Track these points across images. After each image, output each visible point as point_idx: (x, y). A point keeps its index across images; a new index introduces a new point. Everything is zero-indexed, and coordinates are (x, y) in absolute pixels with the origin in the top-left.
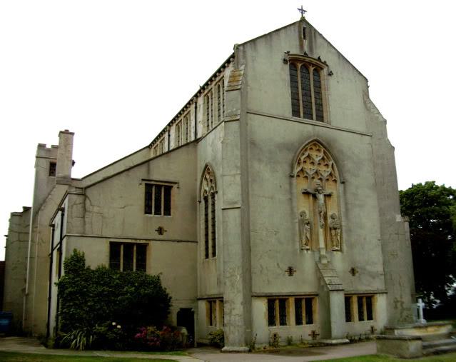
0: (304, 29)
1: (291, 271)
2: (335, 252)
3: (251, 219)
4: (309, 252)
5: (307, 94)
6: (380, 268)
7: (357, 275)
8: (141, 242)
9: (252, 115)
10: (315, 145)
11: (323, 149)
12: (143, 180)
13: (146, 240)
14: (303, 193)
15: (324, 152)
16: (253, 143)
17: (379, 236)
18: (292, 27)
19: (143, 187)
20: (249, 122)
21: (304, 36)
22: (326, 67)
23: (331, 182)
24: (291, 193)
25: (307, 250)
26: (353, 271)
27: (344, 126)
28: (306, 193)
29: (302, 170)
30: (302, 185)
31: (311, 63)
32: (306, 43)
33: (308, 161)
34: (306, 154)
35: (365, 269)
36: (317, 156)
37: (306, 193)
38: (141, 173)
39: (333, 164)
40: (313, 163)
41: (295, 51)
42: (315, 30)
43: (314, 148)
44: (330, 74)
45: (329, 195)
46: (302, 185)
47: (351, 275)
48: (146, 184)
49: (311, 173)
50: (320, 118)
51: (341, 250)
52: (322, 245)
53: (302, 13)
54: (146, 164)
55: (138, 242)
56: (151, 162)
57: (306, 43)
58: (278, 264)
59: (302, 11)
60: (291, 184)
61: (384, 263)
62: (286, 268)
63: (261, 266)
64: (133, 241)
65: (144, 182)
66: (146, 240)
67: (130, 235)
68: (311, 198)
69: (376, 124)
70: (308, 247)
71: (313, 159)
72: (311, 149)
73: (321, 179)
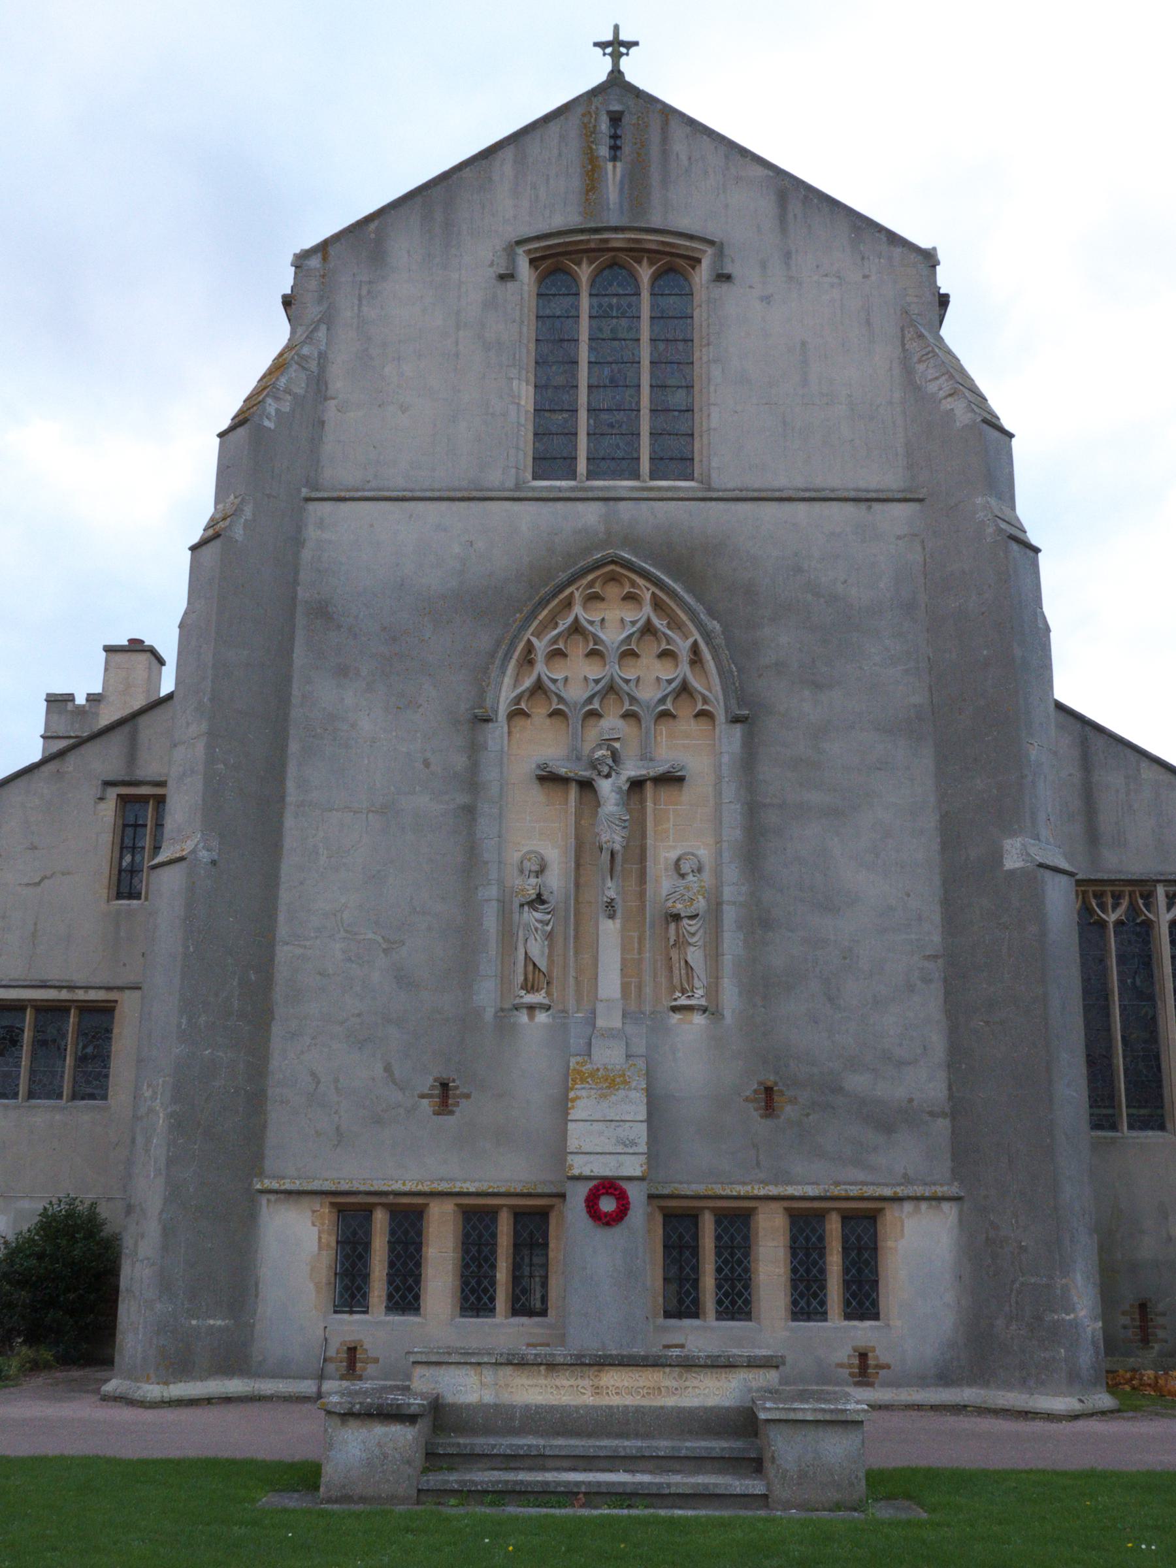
0: (618, 122)
1: (445, 1095)
2: (677, 1017)
3: (285, 896)
4: (542, 1017)
5: (615, 378)
6: (927, 1083)
7: (789, 1111)
8: (93, 995)
9: (328, 506)
10: (613, 578)
11: (647, 593)
12: (108, 784)
13: (109, 989)
14: (542, 779)
15: (657, 605)
16: (323, 612)
17: (937, 939)
18: (554, 127)
19: (108, 810)
20: (312, 533)
21: (615, 148)
22: (710, 251)
23: (687, 725)
24: (471, 781)
25: (531, 1008)
26: (768, 1099)
27: (781, 479)
28: (549, 779)
29: (539, 688)
30: (542, 744)
31: (638, 252)
32: (613, 174)
33: (577, 650)
34: (564, 624)
35: (839, 1090)
36: (613, 622)
37: (549, 779)
38: (104, 760)
39: (695, 644)
40: (593, 654)
41: (560, 214)
42: (668, 113)
43: (613, 592)
44: (724, 278)
45: (672, 779)
46: (542, 744)
47: (755, 1115)
48: (123, 799)
49: (576, 693)
50: (676, 459)
51: (710, 1010)
52: (610, 983)
53: (616, 57)
54: (126, 729)
55: (80, 995)
56: (143, 721)
57: (613, 174)
58: (388, 1069)
59: (617, 47)
60: (474, 749)
61: (958, 1058)
62: (426, 1083)
63: (313, 1074)
64: (64, 995)
65: (112, 793)
66: (109, 989)
67: (53, 974)
68: (573, 792)
69: (959, 452)
70: (530, 998)
71: (597, 640)
72: (596, 598)
73: (628, 715)
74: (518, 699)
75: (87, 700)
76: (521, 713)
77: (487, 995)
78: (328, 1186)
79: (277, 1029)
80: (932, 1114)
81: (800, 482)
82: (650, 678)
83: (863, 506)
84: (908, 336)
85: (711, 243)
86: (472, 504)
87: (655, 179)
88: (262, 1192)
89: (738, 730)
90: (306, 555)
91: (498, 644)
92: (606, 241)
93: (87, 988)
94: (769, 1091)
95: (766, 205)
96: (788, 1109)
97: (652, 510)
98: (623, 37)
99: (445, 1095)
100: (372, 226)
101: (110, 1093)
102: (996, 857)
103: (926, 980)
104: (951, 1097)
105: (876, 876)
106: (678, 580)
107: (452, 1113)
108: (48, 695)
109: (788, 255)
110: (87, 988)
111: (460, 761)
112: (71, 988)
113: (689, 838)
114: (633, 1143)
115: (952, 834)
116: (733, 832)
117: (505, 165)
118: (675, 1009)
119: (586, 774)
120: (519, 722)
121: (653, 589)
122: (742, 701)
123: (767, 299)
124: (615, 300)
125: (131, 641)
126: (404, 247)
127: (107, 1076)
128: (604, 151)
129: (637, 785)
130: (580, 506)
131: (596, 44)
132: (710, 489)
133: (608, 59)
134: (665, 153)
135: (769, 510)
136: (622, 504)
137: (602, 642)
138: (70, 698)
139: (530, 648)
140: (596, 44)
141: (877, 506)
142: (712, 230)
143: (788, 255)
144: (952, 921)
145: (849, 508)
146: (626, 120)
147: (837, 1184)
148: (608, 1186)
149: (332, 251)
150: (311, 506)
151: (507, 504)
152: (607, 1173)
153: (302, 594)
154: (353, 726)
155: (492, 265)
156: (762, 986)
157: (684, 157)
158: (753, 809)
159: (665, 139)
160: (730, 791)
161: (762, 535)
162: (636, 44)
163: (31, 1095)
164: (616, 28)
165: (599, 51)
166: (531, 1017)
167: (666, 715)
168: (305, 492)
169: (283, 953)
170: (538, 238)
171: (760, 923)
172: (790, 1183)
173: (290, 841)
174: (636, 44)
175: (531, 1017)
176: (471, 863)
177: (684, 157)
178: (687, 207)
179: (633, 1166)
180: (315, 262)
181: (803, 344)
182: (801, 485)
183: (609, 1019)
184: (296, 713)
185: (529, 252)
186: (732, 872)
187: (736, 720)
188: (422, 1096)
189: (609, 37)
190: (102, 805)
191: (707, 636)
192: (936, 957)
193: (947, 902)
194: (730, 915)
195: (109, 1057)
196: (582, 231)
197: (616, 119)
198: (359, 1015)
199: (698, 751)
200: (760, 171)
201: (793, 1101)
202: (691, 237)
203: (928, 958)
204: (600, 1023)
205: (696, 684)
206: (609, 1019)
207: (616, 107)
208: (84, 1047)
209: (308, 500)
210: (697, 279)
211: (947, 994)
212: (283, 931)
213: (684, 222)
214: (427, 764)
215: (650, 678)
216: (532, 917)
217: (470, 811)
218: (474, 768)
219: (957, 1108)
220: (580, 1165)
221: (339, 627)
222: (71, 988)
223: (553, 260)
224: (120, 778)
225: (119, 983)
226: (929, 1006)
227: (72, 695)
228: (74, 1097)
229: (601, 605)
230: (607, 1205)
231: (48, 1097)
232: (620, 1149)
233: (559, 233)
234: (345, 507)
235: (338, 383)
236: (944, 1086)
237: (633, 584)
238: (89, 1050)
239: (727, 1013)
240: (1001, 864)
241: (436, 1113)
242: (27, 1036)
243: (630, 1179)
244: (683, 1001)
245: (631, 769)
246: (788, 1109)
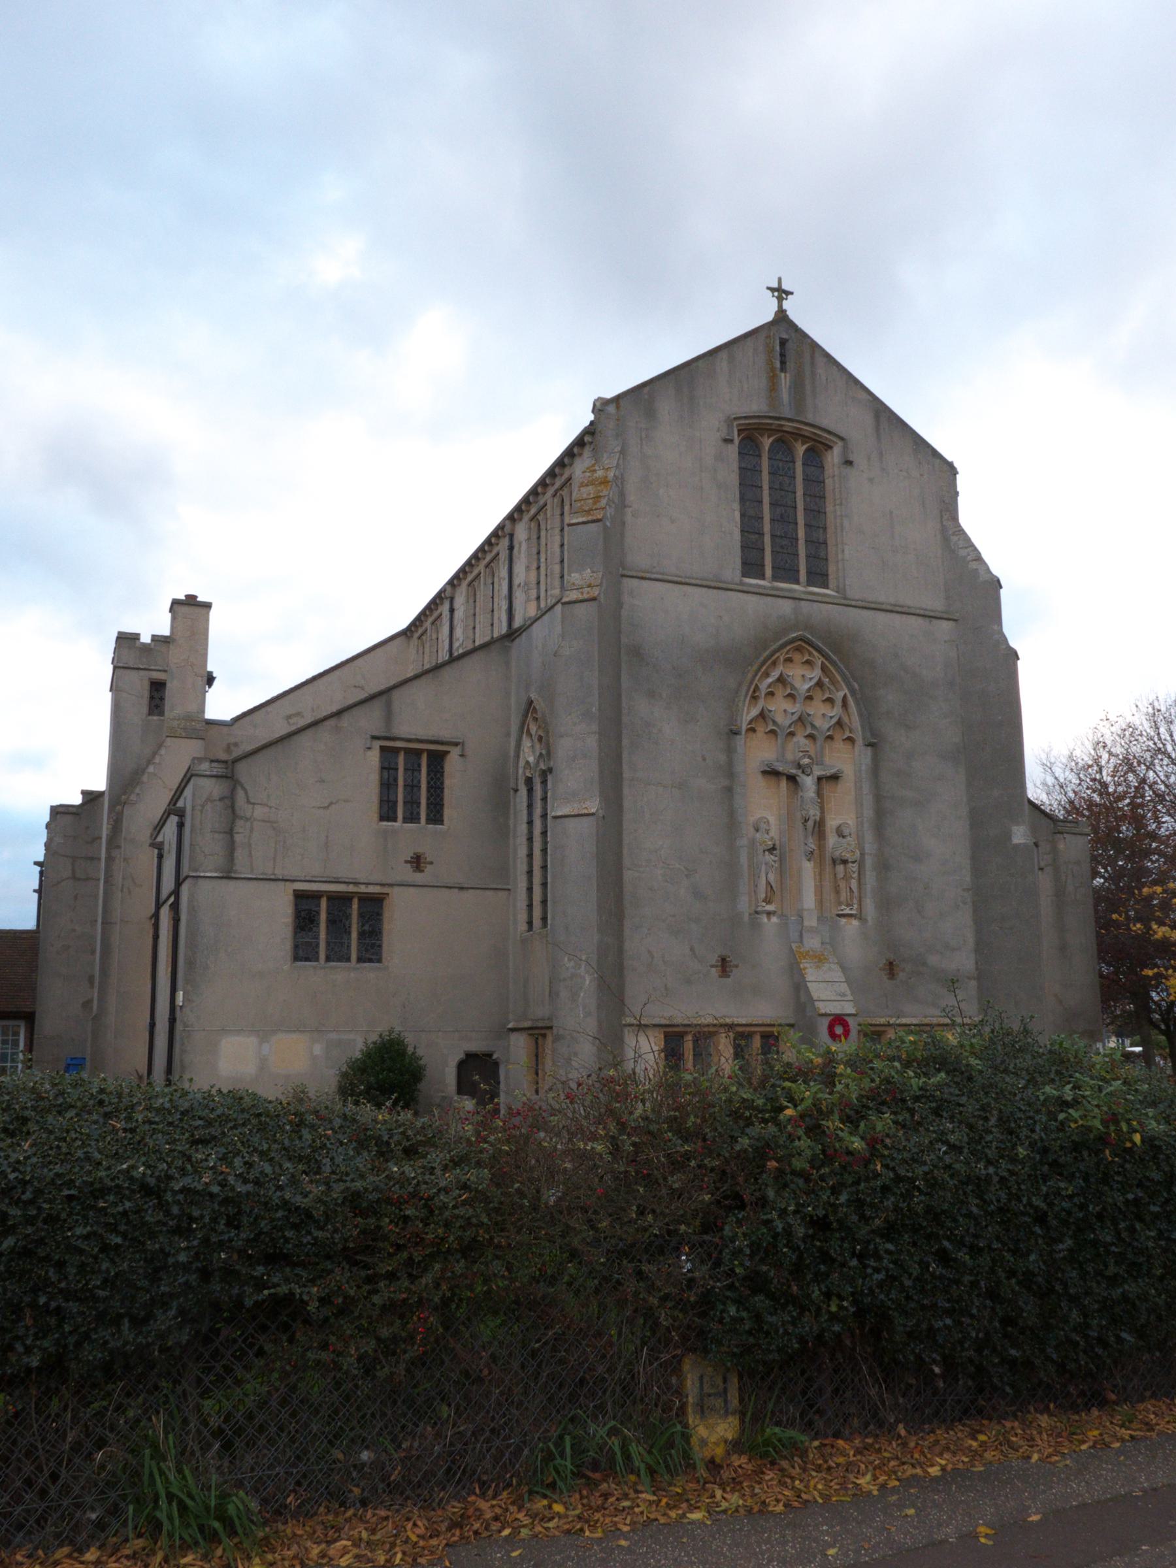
0: (782, 346)
1: (724, 966)
2: (844, 920)
3: (626, 839)
4: (774, 919)
5: (784, 518)
6: (964, 961)
7: (902, 976)
8: (372, 889)
9: (635, 582)
10: (798, 649)
11: (819, 661)
12: (374, 738)
13: (382, 885)
14: (764, 773)
15: (824, 669)
16: (637, 652)
17: (968, 879)
18: (749, 342)
19: (374, 757)
20: (626, 598)
21: (783, 363)
22: (840, 443)
23: (838, 744)
24: (729, 771)
25: (769, 914)
26: (891, 969)
27: (883, 596)
28: (771, 773)
29: (762, 715)
30: (759, 752)
31: (798, 435)
32: (785, 380)
33: (780, 692)
34: (775, 675)
35: (924, 964)
36: (802, 677)
37: (771, 773)
38: (370, 720)
39: (845, 696)
40: (791, 696)
41: (756, 406)
42: (815, 346)
43: (797, 657)
44: (849, 463)
45: (835, 778)
46: (759, 752)
47: (885, 978)
48: (383, 749)
49: (783, 721)
50: (819, 576)
51: (860, 916)
52: (809, 900)
53: (780, 300)
54: (384, 698)
55: (363, 889)
56: (395, 694)
57: (785, 380)
58: (692, 949)
59: (781, 293)
60: (730, 751)
61: (981, 947)
62: (714, 959)
63: (649, 952)
64: (351, 888)
65: (377, 744)
66: (382, 885)
67: (342, 872)
68: (784, 783)
69: (972, 594)
70: (770, 908)
71: (793, 687)
72: (790, 660)
73: (811, 737)
74: (750, 722)
75: (152, 640)
76: (753, 730)
77: (744, 905)
78: (663, 1022)
79: (627, 923)
80: (969, 978)
81: (892, 600)
82: (822, 715)
83: (927, 620)
84: (945, 517)
85: (842, 439)
86: (720, 592)
87: (808, 387)
88: (625, 1025)
89: (869, 750)
90: (624, 613)
91: (740, 684)
92: (782, 426)
93: (367, 884)
94: (891, 963)
95: (869, 419)
96: (901, 974)
97: (815, 606)
98: (784, 287)
99: (724, 966)
100: (646, 390)
101: (384, 955)
102: (1008, 836)
103: (965, 903)
104: (977, 969)
105: (940, 841)
106: (832, 651)
107: (729, 976)
108: (119, 633)
109: (881, 455)
110: (367, 884)
111: (722, 758)
112: (356, 884)
113: (845, 812)
114: (844, 995)
115: (976, 820)
116: (868, 812)
117: (722, 363)
118: (839, 916)
119: (794, 771)
120: (751, 734)
121: (822, 659)
122: (873, 735)
123: (871, 480)
124: (781, 464)
125: (187, 596)
126: (666, 407)
127: (380, 946)
128: (778, 365)
129: (820, 779)
130: (780, 601)
131: (768, 288)
132: (845, 598)
133: (775, 301)
134: (813, 374)
135: (881, 616)
136: (803, 603)
137: (795, 689)
138: (135, 637)
139: (757, 688)
140: (768, 288)
141: (935, 621)
142: (841, 431)
143: (881, 455)
144: (978, 869)
145: (920, 620)
146: (789, 345)
147: (926, 1017)
148: (839, 1020)
149: (622, 403)
150: (625, 580)
151: (740, 594)
152: (838, 1012)
153: (624, 640)
154: (660, 731)
155: (718, 430)
156: (886, 904)
157: (824, 378)
158: (878, 798)
159: (813, 364)
160: (866, 787)
161: (878, 629)
162: (792, 293)
163: (328, 959)
164: (780, 280)
165: (769, 293)
166: (769, 919)
167: (830, 738)
168: (621, 571)
169: (628, 875)
170: (745, 418)
171: (884, 867)
172: (904, 1016)
173: (627, 804)
174: (792, 293)
175: (769, 919)
176: (732, 823)
177: (824, 378)
178: (828, 413)
179: (849, 1009)
180: (611, 409)
181: (891, 513)
182: (893, 602)
183: (811, 921)
184: (625, 719)
185: (739, 425)
186: (869, 837)
187: (870, 745)
188: (712, 966)
189: (776, 285)
190: (369, 753)
191: (853, 692)
192: (968, 890)
193: (973, 858)
194: (869, 862)
195: (381, 933)
196: (770, 418)
197: (783, 343)
198: (674, 916)
199: (846, 759)
200: (865, 396)
201: (903, 970)
202: (829, 432)
203: (964, 890)
204: (806, 923)
205: (846, 719)
206: (811, 921)
207: (785, 336)
208: (363, 925)
209: (623, 576)
210: (829, 459)
211: (975, 911)
212: (627, 861)
213: (825, 422)
214: (704, 759)
215: (822, 715)
216: (769, 858)
217: (729, 790)
218: (730, 763)
219: (981, 976)
220: (824, 1008)
221: (648, 664)
222: (356, 884)
223: (749, 434)
224: (383, 734)
225: (389, 881)
226: (965, 917)
227: (138, 635)
228: (359, 960)
229: (791, 665)
230: (839, 1030)
231: (339, 960)
232: (839, 998)
233: (759, 417)
234: (645, 583)
235: (631, 498)
236: (973, 962)
237: (810, 654)
238: (366, 927)
239: (869, 918)
240: (1010, 838)
241: (720, 977)
242: (323, 916)
243: (849, 1015)
244: (847, 911)
245: (818, 772)
246: (901, 974)
